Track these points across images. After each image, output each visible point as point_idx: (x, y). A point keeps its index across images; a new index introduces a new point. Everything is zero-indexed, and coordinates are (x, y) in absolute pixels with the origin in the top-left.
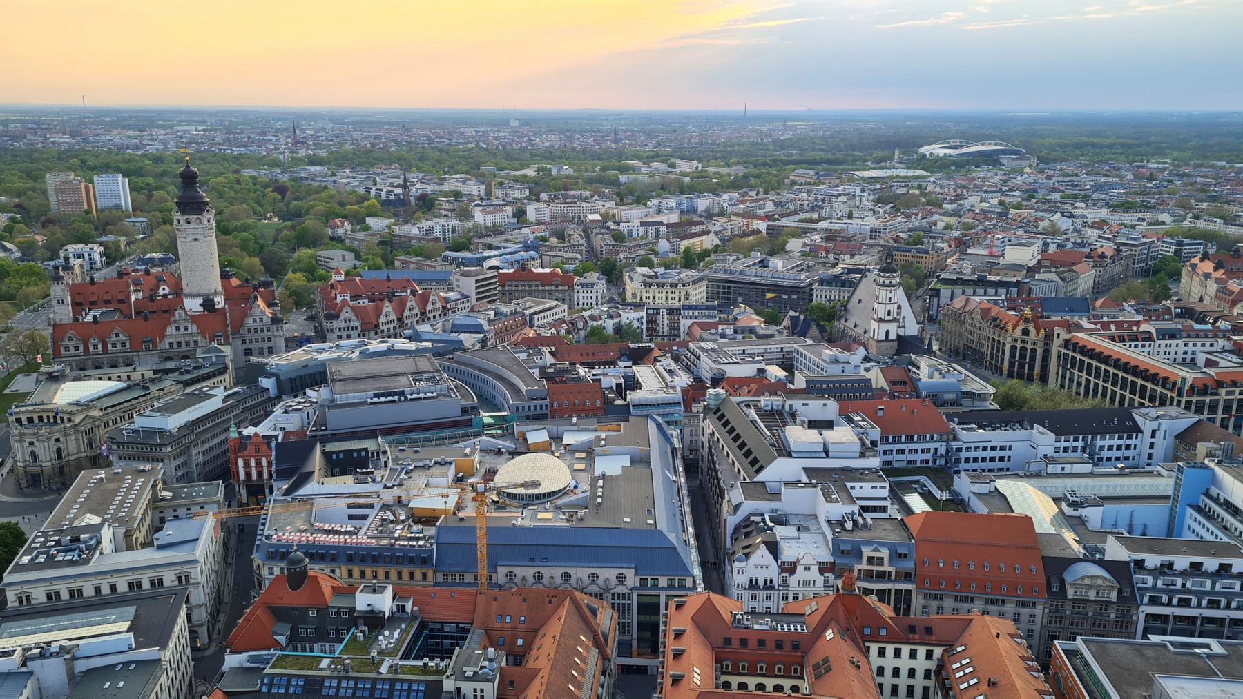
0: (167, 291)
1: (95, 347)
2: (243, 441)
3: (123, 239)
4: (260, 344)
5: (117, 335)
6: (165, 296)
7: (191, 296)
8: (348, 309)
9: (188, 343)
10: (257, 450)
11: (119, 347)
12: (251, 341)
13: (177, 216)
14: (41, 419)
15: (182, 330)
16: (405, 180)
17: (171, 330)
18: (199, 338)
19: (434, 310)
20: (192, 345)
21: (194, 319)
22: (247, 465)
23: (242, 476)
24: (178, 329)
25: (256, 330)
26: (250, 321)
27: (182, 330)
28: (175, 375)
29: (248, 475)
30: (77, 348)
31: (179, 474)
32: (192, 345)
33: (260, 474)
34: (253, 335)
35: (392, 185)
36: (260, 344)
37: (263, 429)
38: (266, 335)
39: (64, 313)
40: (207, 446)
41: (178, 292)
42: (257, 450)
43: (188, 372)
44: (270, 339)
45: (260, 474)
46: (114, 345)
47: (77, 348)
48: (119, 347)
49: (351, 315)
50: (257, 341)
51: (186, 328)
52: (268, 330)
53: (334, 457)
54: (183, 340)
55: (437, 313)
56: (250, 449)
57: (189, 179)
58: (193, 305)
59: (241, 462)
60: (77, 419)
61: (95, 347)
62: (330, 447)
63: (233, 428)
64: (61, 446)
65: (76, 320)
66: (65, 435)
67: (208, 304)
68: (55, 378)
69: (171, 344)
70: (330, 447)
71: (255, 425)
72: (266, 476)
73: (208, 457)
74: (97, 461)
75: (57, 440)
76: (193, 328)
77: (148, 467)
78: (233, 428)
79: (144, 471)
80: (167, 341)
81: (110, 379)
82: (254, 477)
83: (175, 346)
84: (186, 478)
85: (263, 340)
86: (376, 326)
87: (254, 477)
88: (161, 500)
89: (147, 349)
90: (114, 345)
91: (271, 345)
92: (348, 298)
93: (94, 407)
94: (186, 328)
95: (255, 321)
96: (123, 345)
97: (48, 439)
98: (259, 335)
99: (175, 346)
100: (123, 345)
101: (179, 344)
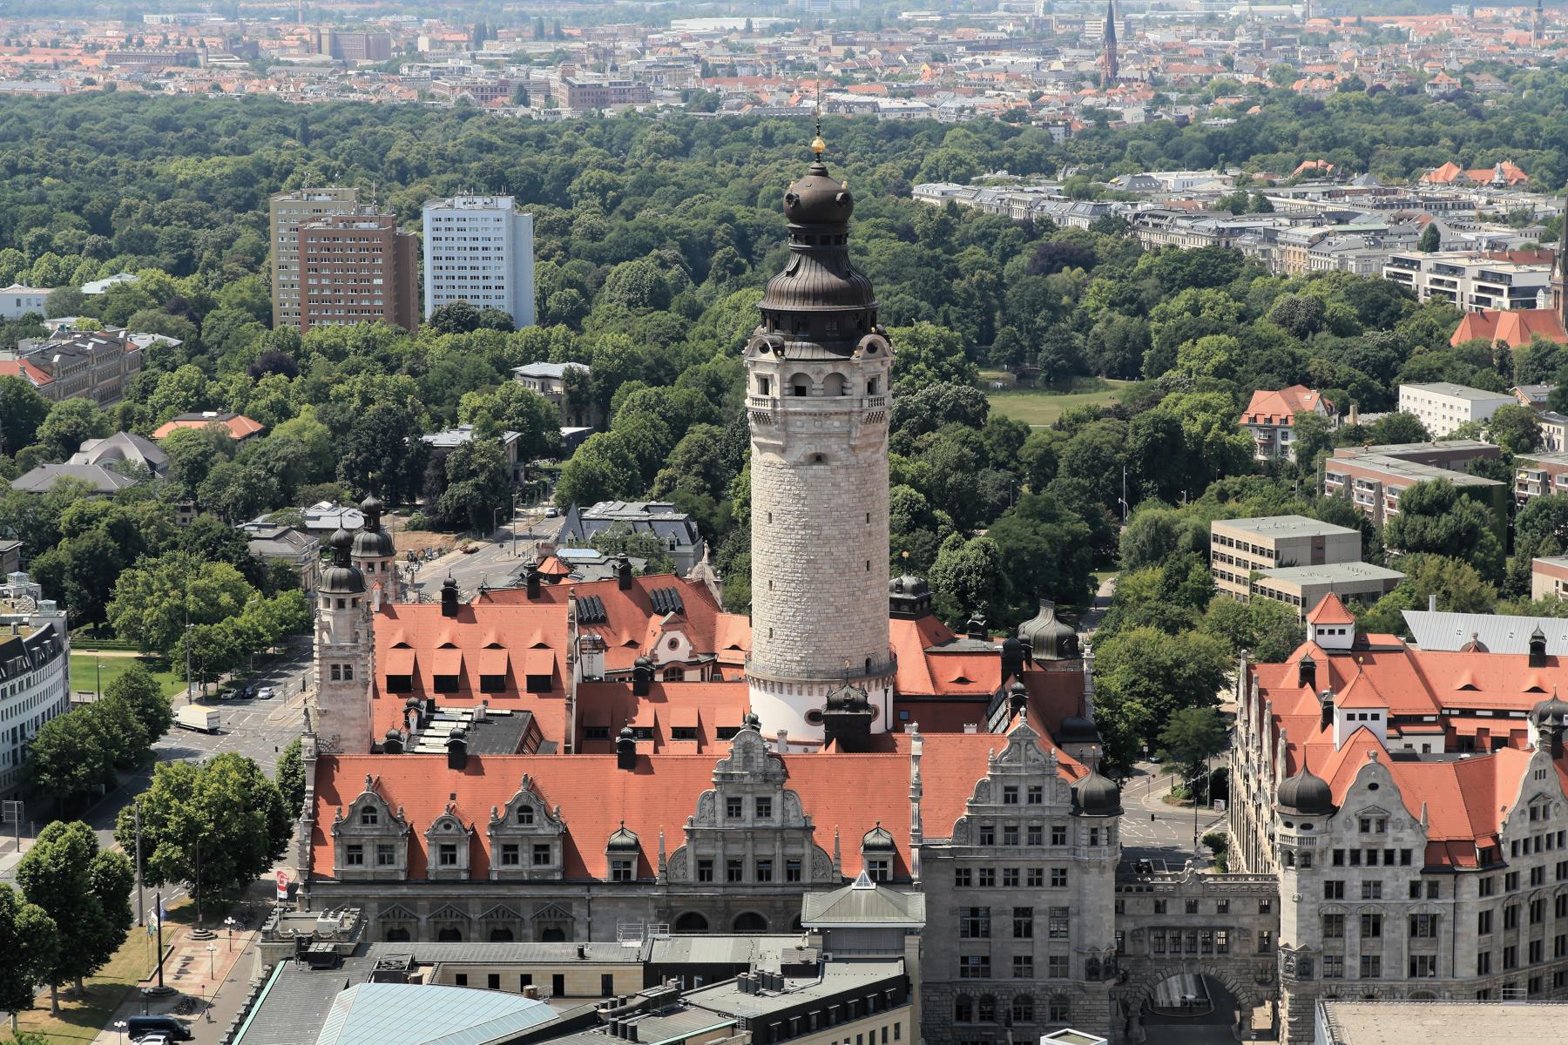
4: (1023, 896)
11: (525, 864)
12: (988, 880)
15: (749, 811)
20: (778, 877)
27: (749, 811)
30: (385, 856)
32: (778, 877)
36: (1023, 896)
38: (1049, 857)
43: (770, 983)
44: (1060, 879)
46: (510, 853)
48: (525, 864)
50: (1012, 879)
51: (763, 807)
52: (1059, 837)
58: (780, 717)
61: (448, 854)
81: (494, 983)
83: (719, 875)
85: (1036, 879)
91: (1063, 897)
94: (763, 807)
98: (1024, 858)
99: (719, 875)
100: (542, 853)
101: (734, 870)
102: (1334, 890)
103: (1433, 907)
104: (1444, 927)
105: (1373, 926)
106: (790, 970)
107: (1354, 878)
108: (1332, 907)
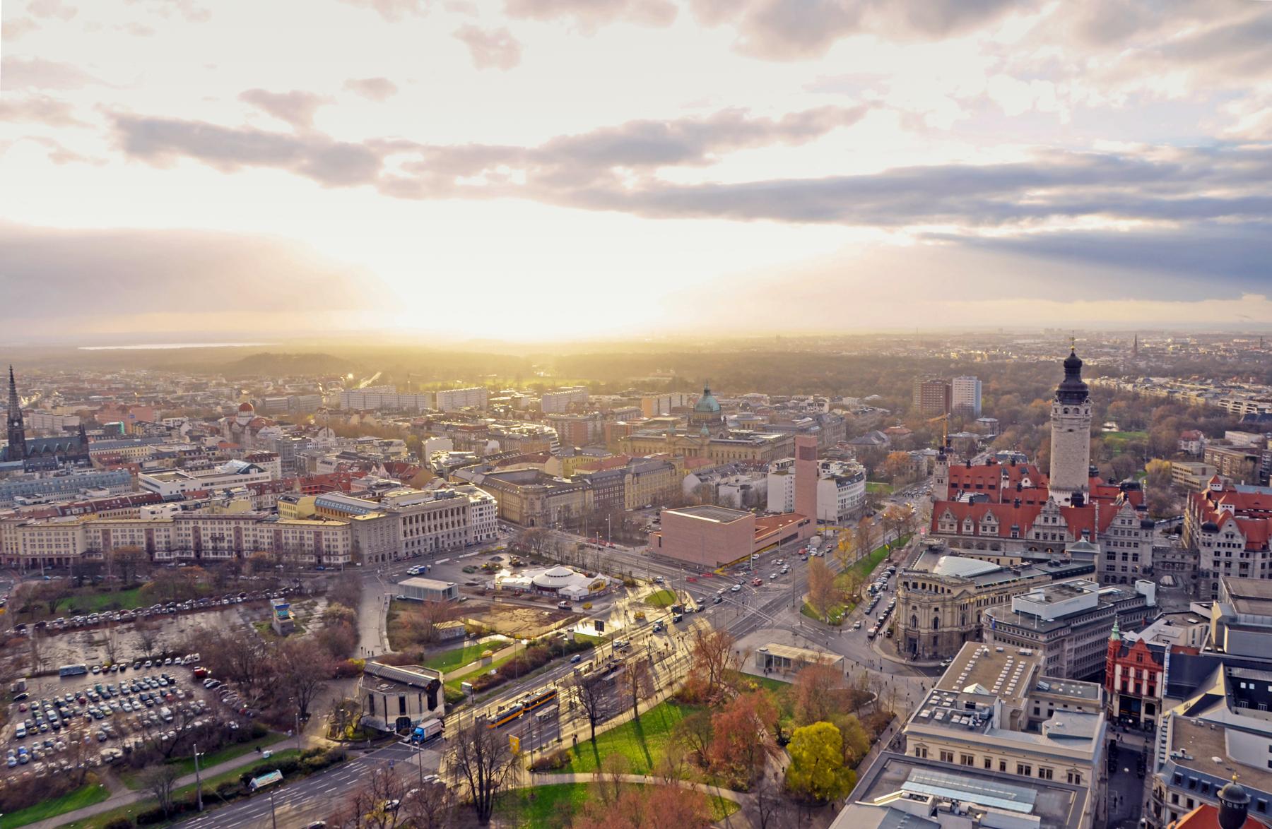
1: (968, 528)
2: (1123, 649)
5: (989, 518)
8: (1233, 523)
10: (1140, 659)
11: (988, 531)
12: (1116, 544)
14: (924, 586)
17: (1039, 520)
18: (1066, 533)
22: (1125, 674)
23: (1118, 686)
24: (1046, 520)
25: (1123, 533)
26: (1117, 522)
28: (1045, 566)
29: (1125, 685)
31: (1051, 667)
33: (1138, 687)
34: (1119, 538)
37: (1147, 636)
38: (1133, 539)
40: (1080, 644)
41: (1039, 486)
42: (1140, 659)
43: (1057, 565)
44: (1136, 545)
45: (1138, 687)
46: (985, 528)
48: (988, 531)
50: (1122, 545)
51: (1054, 520)
52: (1136, 534)
53: (1243, 685)
54: (1049, 532)
56: (1131, 657)
57: (1073, 366)
59: (1118, 669)
60: (956, 592)
61: (968, 528)
62: (1237, 672)
63: (1115, 629)
64: (940, 617)
66: (944, 606)
68: (935, 551)
69: (1037, 535)
70: (1237, 672)
71: (1137, 631)
72: (1144, 691)
73: (1079, 657)
74: (978, 635)
75: (936, 609)
76: (1061, 521)
77: (1029, 651)
78: (1115, 629)
79: (1024, 654)
82: (1131, 689)
83: (1041, 538)
84: (1055, 672)
85: (1129, 545)
87: (1131, 689)
88: (1039, 689)
89: (1014, 537)
90: (985, 528)
93: (972, 583)
94: (1054, 520)
95: (1123, 522)
96: (993, 529)
97: (929, 607)
98: (1126, 538)
102: (1217, 554)
103: (1248, 560)
104: (1250, 567)
105: (1228, 565)
106: (1062, 562)
107: (1223, 551)
108: (1216, 558)
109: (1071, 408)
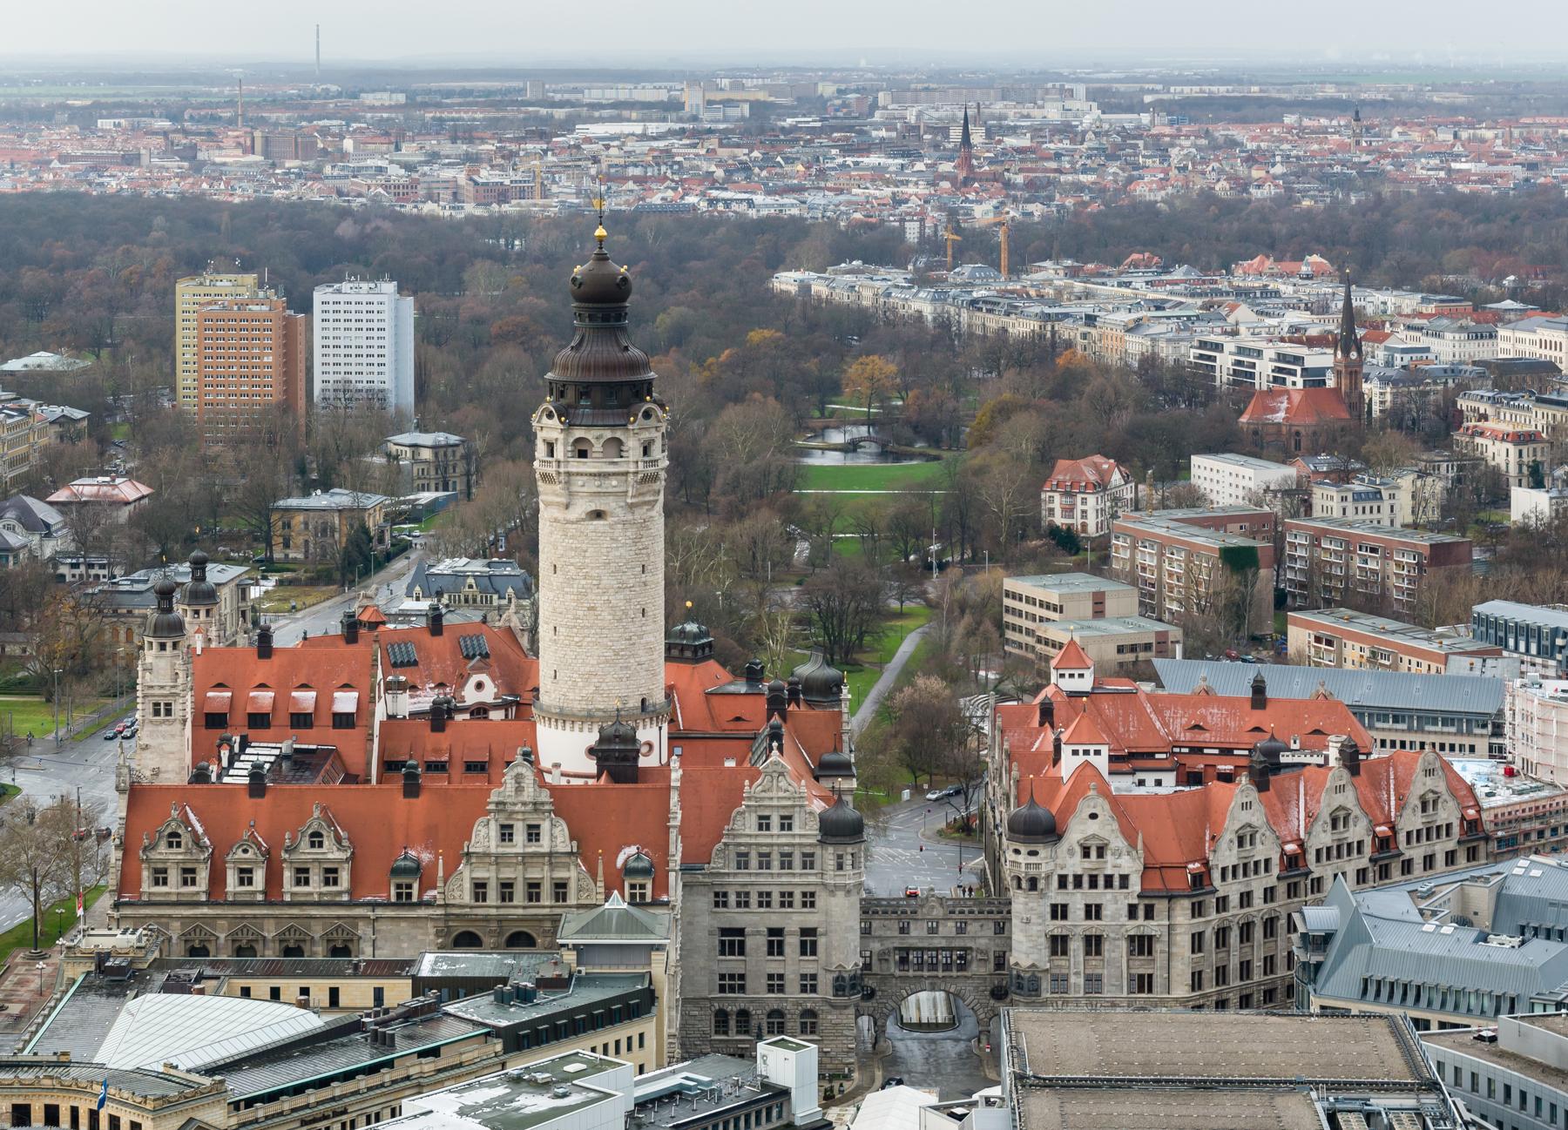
0: (489, 695)
1: (245, 876)
3: (373, 500)
6: (480, 711)
7: (564, 717)
8: (1102, 807)
9: (533, 889)
13: (548, 428)
16: (1351, 316)
17: (485, 836)
18: (572, 874)
19: (1431, 832)
21: (564, 802)
24: (506, 833)
25: (765, 862)
30: (188, 875)
34: (756, 879)
35: (1297, 335)
38: (799, 880)
39: (166, 752)
41: (520, 701)
44: (809, 900)
46: (302, 876)
47: (188, 875)
49: (1106, 829)
52: (808, 861)
55: (1441, 847)
61: (245, 876)
65: (200, 776)
67: (616, 756)
68: (116, 978)
69: (480, 887)
76: (556, 836)
80: (466, 875)
85: (787, 900)
86: (1200, 880)
89: (404, 900)
90: (302, 876)
92: (1102, 763)
96: (330, 876)
98: (776, 880)
100: (330, 876)
109: (595, 437)
